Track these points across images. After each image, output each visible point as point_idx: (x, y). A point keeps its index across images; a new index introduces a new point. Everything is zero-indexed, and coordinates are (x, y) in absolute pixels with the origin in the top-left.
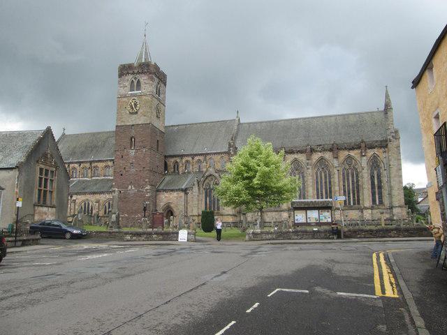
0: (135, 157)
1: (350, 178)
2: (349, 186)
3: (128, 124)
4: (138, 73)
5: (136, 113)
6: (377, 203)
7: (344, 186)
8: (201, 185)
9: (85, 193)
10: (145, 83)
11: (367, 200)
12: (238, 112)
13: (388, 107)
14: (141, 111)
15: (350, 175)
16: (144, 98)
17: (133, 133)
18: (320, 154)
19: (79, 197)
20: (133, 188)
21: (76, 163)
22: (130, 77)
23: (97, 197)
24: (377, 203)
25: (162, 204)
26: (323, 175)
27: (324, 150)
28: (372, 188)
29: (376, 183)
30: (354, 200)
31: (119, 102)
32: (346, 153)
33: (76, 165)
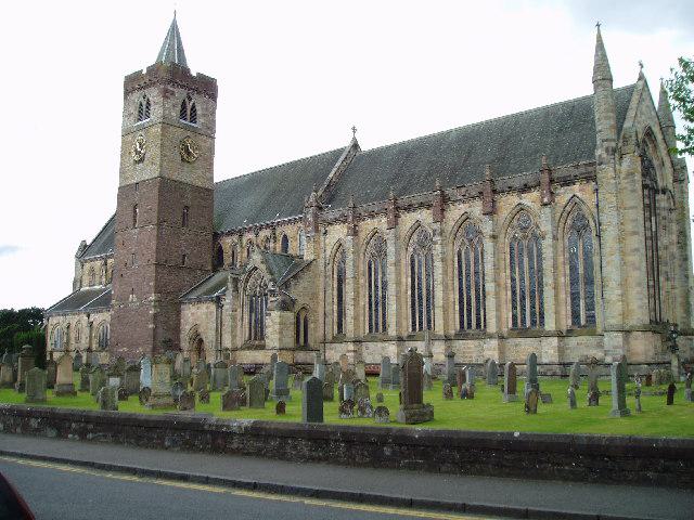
0: (139, 243)
1: (526, 260)
2: (522, 279)
7: (513, 280)
8: (241, 286)
11: (497, 314)
13: (641, 77)
15: (525, 253)
18: (463, 208)
24: (583, 322)
25: (188, 327)
26: (472, 255)
29: (581, 271)
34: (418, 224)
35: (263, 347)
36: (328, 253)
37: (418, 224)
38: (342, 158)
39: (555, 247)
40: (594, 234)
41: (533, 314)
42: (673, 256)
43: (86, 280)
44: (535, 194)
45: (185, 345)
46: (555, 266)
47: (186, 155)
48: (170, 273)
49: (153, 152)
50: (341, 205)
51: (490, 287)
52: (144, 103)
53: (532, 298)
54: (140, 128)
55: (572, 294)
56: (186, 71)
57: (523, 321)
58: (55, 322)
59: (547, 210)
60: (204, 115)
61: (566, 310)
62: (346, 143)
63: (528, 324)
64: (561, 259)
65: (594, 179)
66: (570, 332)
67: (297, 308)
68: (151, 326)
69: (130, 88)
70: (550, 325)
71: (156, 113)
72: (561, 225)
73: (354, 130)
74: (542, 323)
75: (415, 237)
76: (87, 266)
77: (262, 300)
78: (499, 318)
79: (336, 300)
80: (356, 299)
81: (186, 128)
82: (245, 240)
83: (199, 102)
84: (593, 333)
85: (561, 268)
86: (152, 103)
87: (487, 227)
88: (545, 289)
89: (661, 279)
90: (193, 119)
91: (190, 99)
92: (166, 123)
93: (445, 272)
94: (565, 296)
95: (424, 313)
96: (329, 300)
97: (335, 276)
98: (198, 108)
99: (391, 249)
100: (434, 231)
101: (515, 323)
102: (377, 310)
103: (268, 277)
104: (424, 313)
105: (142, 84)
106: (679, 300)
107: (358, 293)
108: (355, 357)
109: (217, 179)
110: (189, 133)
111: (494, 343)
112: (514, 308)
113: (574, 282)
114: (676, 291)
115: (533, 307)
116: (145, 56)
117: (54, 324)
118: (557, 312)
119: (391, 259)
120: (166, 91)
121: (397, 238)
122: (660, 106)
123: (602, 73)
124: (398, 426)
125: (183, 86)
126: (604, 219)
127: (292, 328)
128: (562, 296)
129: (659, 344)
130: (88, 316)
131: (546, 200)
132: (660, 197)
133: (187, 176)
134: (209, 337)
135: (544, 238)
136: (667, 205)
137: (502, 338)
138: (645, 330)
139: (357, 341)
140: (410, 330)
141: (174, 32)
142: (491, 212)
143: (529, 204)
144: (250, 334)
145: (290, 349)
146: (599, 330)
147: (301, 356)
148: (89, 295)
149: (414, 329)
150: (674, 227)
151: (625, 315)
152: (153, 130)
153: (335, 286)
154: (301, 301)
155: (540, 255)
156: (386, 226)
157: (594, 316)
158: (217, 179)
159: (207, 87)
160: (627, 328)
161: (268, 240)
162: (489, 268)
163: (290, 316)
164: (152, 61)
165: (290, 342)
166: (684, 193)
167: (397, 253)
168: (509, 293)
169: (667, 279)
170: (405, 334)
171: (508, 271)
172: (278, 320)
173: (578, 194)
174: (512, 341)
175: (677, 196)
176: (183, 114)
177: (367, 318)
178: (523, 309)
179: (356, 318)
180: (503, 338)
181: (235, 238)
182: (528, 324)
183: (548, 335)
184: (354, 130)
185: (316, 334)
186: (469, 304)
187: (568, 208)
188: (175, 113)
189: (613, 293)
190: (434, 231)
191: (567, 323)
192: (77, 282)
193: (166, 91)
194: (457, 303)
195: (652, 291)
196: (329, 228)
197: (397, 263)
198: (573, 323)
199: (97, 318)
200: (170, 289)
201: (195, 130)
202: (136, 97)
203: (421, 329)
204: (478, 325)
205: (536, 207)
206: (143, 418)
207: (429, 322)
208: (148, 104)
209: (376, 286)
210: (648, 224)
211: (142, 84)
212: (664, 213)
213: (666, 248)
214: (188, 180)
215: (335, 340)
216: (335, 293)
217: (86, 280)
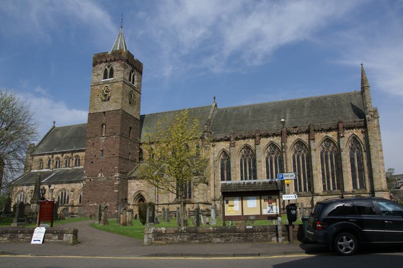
0: (105, 145)
3: (100, 111)
4: (111, 61)
5: (109, 99)
6: (359, 188)
9: (62, 183)
10: (118, 71)
12: (214, 98)
14: (112, 97)
16: (116, 84)
17: (104, 119)
18: (296, 137)
19: (57, 186)
20: (103, 176)
21: (59, 153)
22: (103, 66)
23: (73, 185)
25: (133, 192)
27: (300, 133)
28: (352, 171)
30: (334, 185)
31: (92, 89)
33: (59, 156)
45: (131, 201)
69: (99, 61)
90: (133, 83)
91: (133, 72)
98: (135, 77)
120: (125, 65)
130: (50, 187)
133: (131, 111)
173: (355, 133)
178: (328, 182)
201: (134, 88)
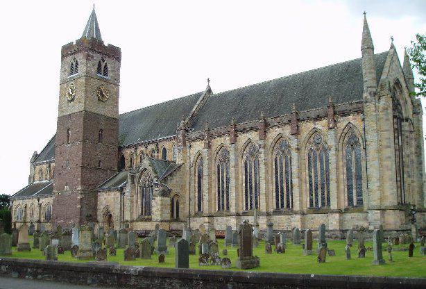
1: (318, 164)
2: (316, 176)
7: (310, 177)
8: (136, 180)
11: (300, 198)
13: (392, 47)
14: (76, 97)
15: (318, 160)
18: (278, 130)
24: (355, 204)
25: (102, 207)
29: (354, 171)
32: (311, 125)
34: (250, 141)
35: (150, 220)
36: (192, 159)
37: (250, 141)
38: (201, 98)
39: (337, 156)
40: (362, 147)
41: (323, 199)
42: (412, 161)
43: (37, 177)
44: (324, 122)
45: (100, 218)
46: (337, 168)
47: (101, 97)
48: (91, 172)
49: (80, 95)
50: (200, 128)
51: (295, 181)
52: (74, 63)
53: (323, 188)
54: (71, 80)
55: (348, 186)
56: (101, 43)
57: (317, 203)
58: (17, 204)
59: (332, 132)
60: (113, 71)
61: (344, 196)
62: (203, 89)
63: (320, 205)
64: (341, 163)
65: (362, 112)
66: (347, 210)
67: (172, 195)
68: (79, 206)
69: (65, 54)
70: (334, 206)
71: (82, 69)
72: (341, 141)
73: (209, 80)
74: (329, 204)
75: (247, 149)
76: (38, 168)
77: (150, 190)
78: (301, 201)
79: (197, 190)
80: (210, 189)
81: (101, 79)
82: (138, 151)
83: (109, 63)
84: (361, 211)
85: (341, 169)
86: (79, 63)
87: (294, 143)
88: (331, 182)
89: (405, 176)
90: (106, 74)
91: (103, 60)
92: (88, 76)
93: (267, 172)
94: (343, 187)
95: (253, 198)
96: (192, 190)
97: (197, 174)
99: (232, 157)
100: (260, 145)
101: (311, 205)
102: (223, 196)
103: (153, 175)
104: (253, 198)
105: (73, 51)
106: (417, 189)
107: (211, 185)
108: (209, 226)
109: (121, 112)
110: (103, 83)
111: (298, 217)
112: (311, 194)
113: (349, 178)
114: (415, 184)
115: (323, 194)
116: (75, 33)
117: (17, 205)
118: (338, 198)
119: (232, 163)
120: (88, 55)
121: (236, 150)
122: (404, 65)
123: (367, 44)
124: (237, 270)
125: (99, 53)
126: (369, 138)
127: (169, 207)
128: (342, 187)
129: (404, 218)
130: (39, 200)
131: (331, 126)
132: (404, 123)
134: (116, 213)
135: (330, 150)
136: (408, 129)
137: (303, 214)
138: (395, 209)
139: (210, 216)
140: (245, 209)
141: (93, 18)
142: (296, 133)
143: (320, 128)
144: (142, 211)
145: (167, 221)
146: (365, 209)
147: (175, 226)
148: (38, 186)
149: (247, 208)
150: (414, 143)
151: (381, 199)
152: (80, 81)
153: (197, 180)
154: (175, 190)
155: (327, 161)
156: (229, 142)
157: (362, 200)
158: (121, 112)
159: (114, 53)
160: (383, 208)
161: (153, 151)
162: (295, 169)
163: (168, 200)
164: (79, 36)
165: (167, 216)
166: (420, 121)
167: (236, 160)
168: (308, 185)
169: (409, 176)
170: (241, 212)
171: (307, 171)
172: (160, 203)
173: (351, 122)
174: (310, 216)
175: (415, 123)
176: (99, 70)
177: (217, 201)
178: (317, 196)
179: (210, 201)
180: (304, 214)
181: (132, 150)
182: (320, 205)
183: (333, 212)
184: (209, 80)
185: (184, 210)
186: (282, 192)
187: (346, 131)
188: (94, 70)
189: (374, 185)
190: (260, 145)
191: (344, 204)
192: (31, 178)
193: (88, 55)
194: (274, 191)
195: (399, 184)
196: (193, 144)
197: (236, 166)
198: (349, 205)
199: (44, 201)
200: (91, 182)
201: (106, 81)
202: (69, 59)
203: (251, 208)
204: (288, 206)
205: (325, 130)
206: (74, 265)
207: (256, 203)
208: (77, 64)
209: (223, 181)
210: (396, 141)
211: (73, 51)
212: (407, 134)
213: (408, 156)
214: (102, 113)
215: (197, 215)
216: (197, 185)
217: (37, 178)
